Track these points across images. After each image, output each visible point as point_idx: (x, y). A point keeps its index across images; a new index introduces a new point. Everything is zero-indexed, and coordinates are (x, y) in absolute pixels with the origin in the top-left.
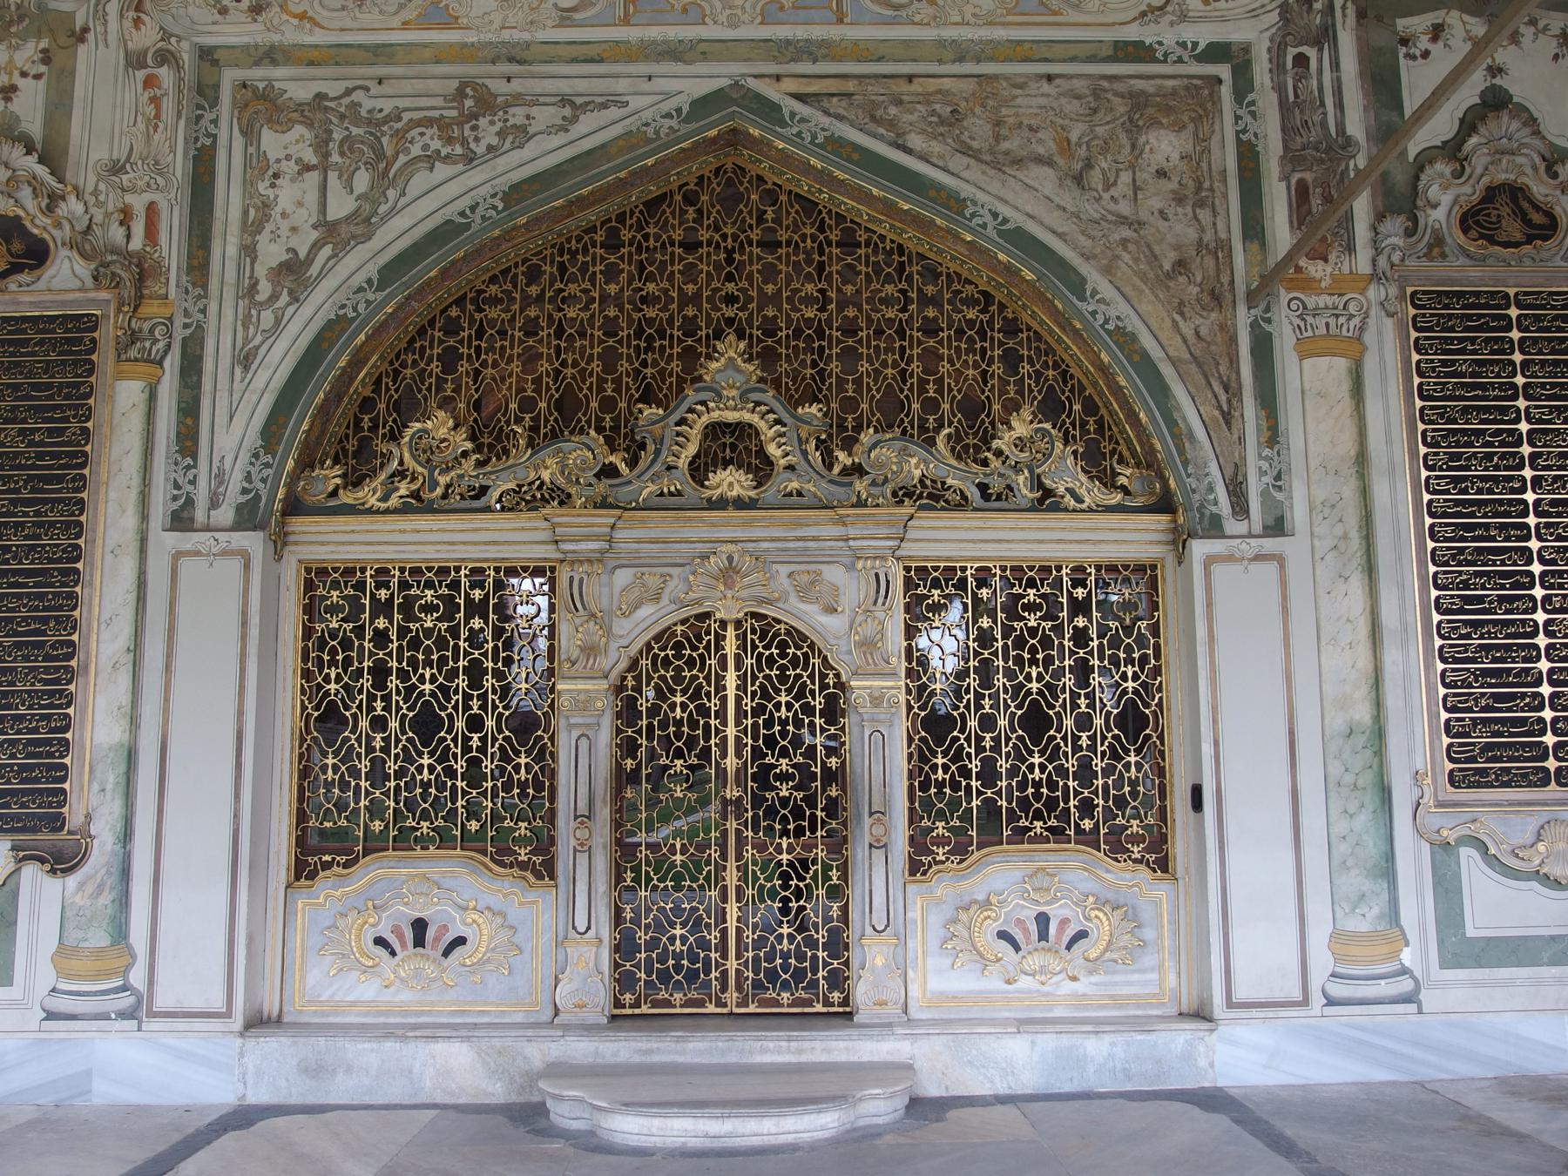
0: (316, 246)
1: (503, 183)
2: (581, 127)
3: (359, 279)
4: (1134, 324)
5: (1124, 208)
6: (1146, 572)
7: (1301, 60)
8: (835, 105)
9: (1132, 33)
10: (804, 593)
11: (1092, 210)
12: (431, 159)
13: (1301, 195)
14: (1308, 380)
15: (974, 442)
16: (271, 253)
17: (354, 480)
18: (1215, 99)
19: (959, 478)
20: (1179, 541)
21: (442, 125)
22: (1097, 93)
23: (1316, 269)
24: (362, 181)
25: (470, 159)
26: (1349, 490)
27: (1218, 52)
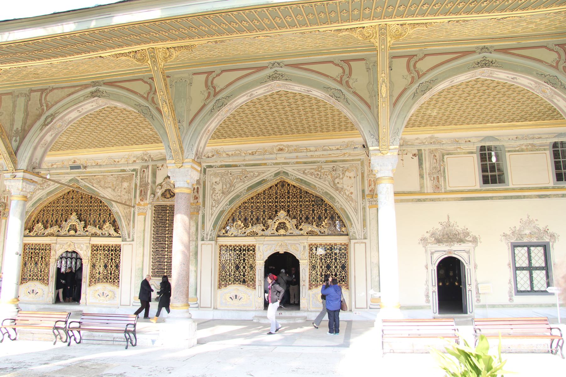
1: (46, 192)
4: (118, 211)
5: (119, 194)
7: (144, 171)
8: (86, 180)
9: (122, 168)
10: (78, 248)
11: (115, 195)
12: (39, 189)
13: (141, 191)
14: (139, 219)
17: (30, 232)
18: (133, 177)
19: (99, 232)
22: (118, 177)
23: (142, 203)
25: (43, 189)
26: (142, 235)
27: (134, 170)
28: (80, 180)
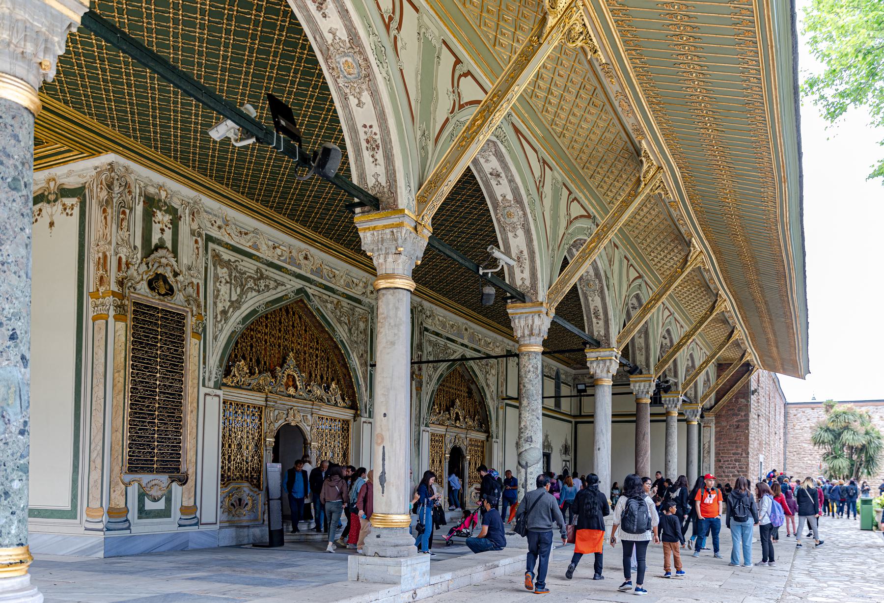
0: (229, 307)
2: (279, 290)
3: (238, 320)
6: (346, 422)
12: (252, 289)
15: (327, 389)
16: (220, 307)
20: (356, 416)
21: (255, 280)
24: (239, 290)
25: (259, 291)
28: (312, 297)
